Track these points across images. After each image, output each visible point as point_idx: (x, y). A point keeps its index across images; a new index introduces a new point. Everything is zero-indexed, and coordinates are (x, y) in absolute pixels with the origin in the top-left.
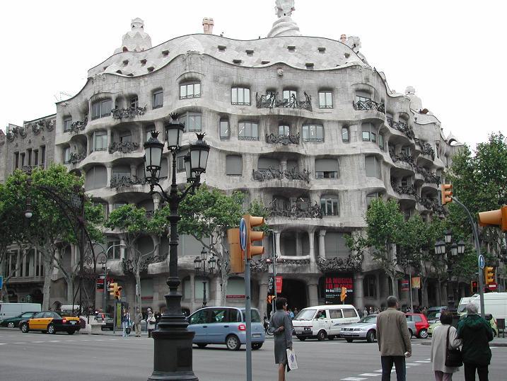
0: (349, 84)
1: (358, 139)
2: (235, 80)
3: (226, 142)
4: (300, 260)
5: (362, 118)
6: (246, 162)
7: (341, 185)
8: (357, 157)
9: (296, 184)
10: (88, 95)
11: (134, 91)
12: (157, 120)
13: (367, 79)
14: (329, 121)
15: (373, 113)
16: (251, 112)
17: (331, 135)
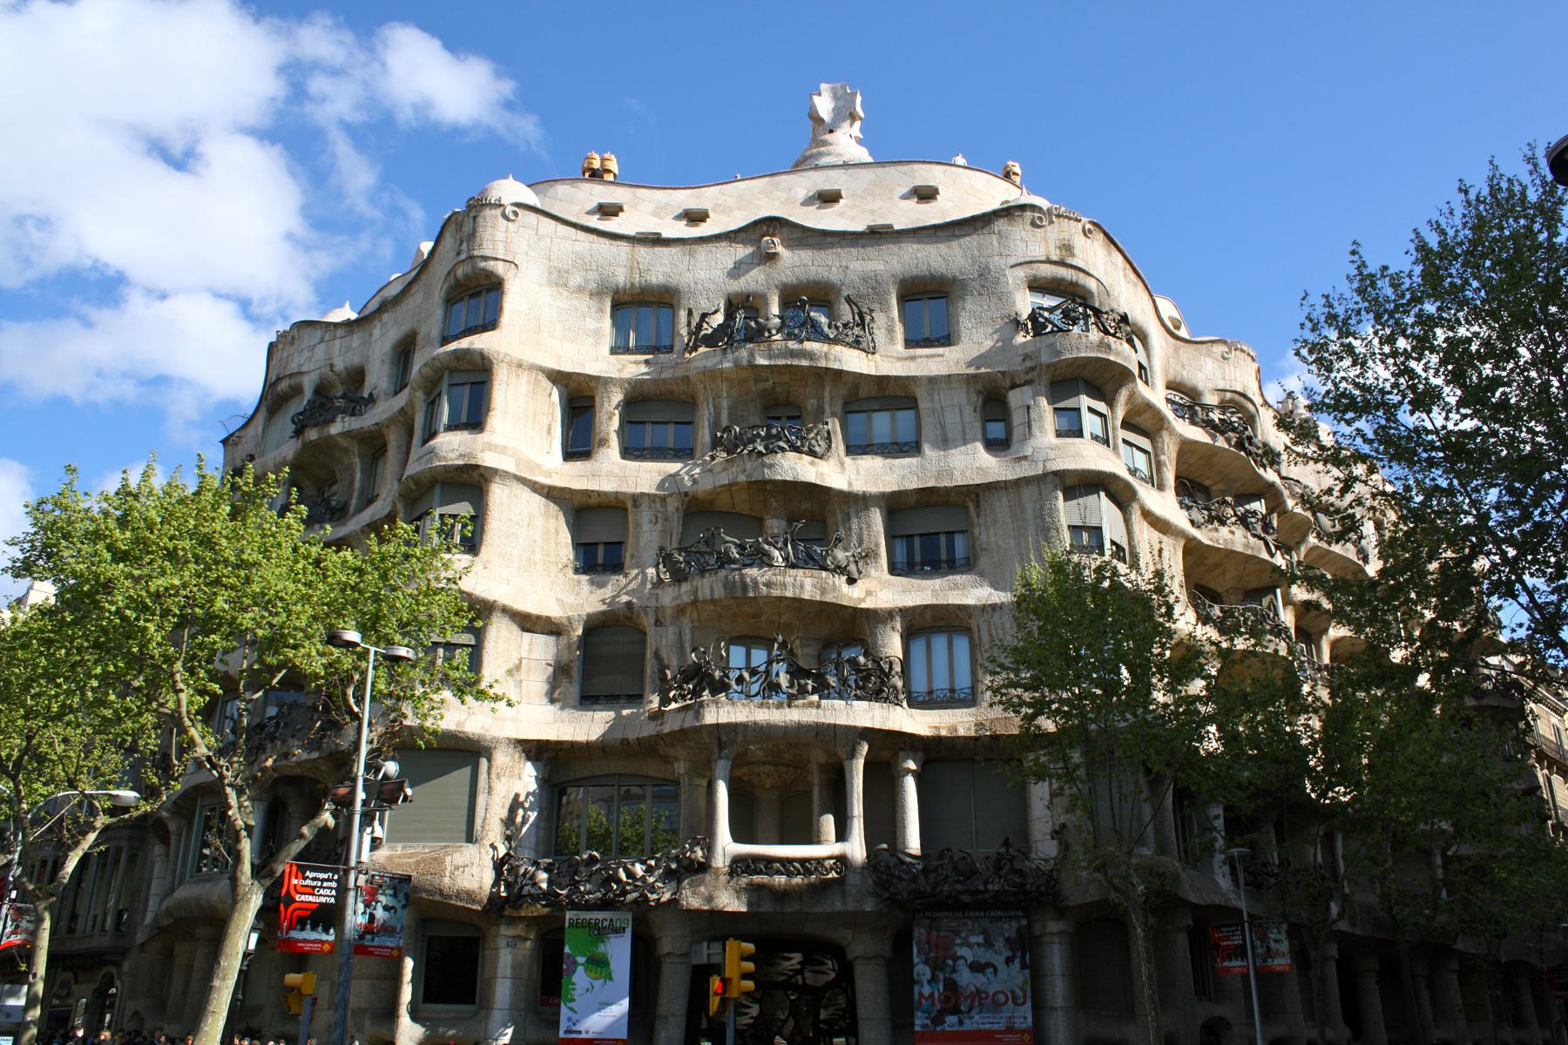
0: (997, 262)
2: (621, 278)
3: (578, 466)
4: (808, 860)
6: (638, 525)
11: (355, 359)
12: (392, 420)
14: (932, 380)
17: (943, 426)
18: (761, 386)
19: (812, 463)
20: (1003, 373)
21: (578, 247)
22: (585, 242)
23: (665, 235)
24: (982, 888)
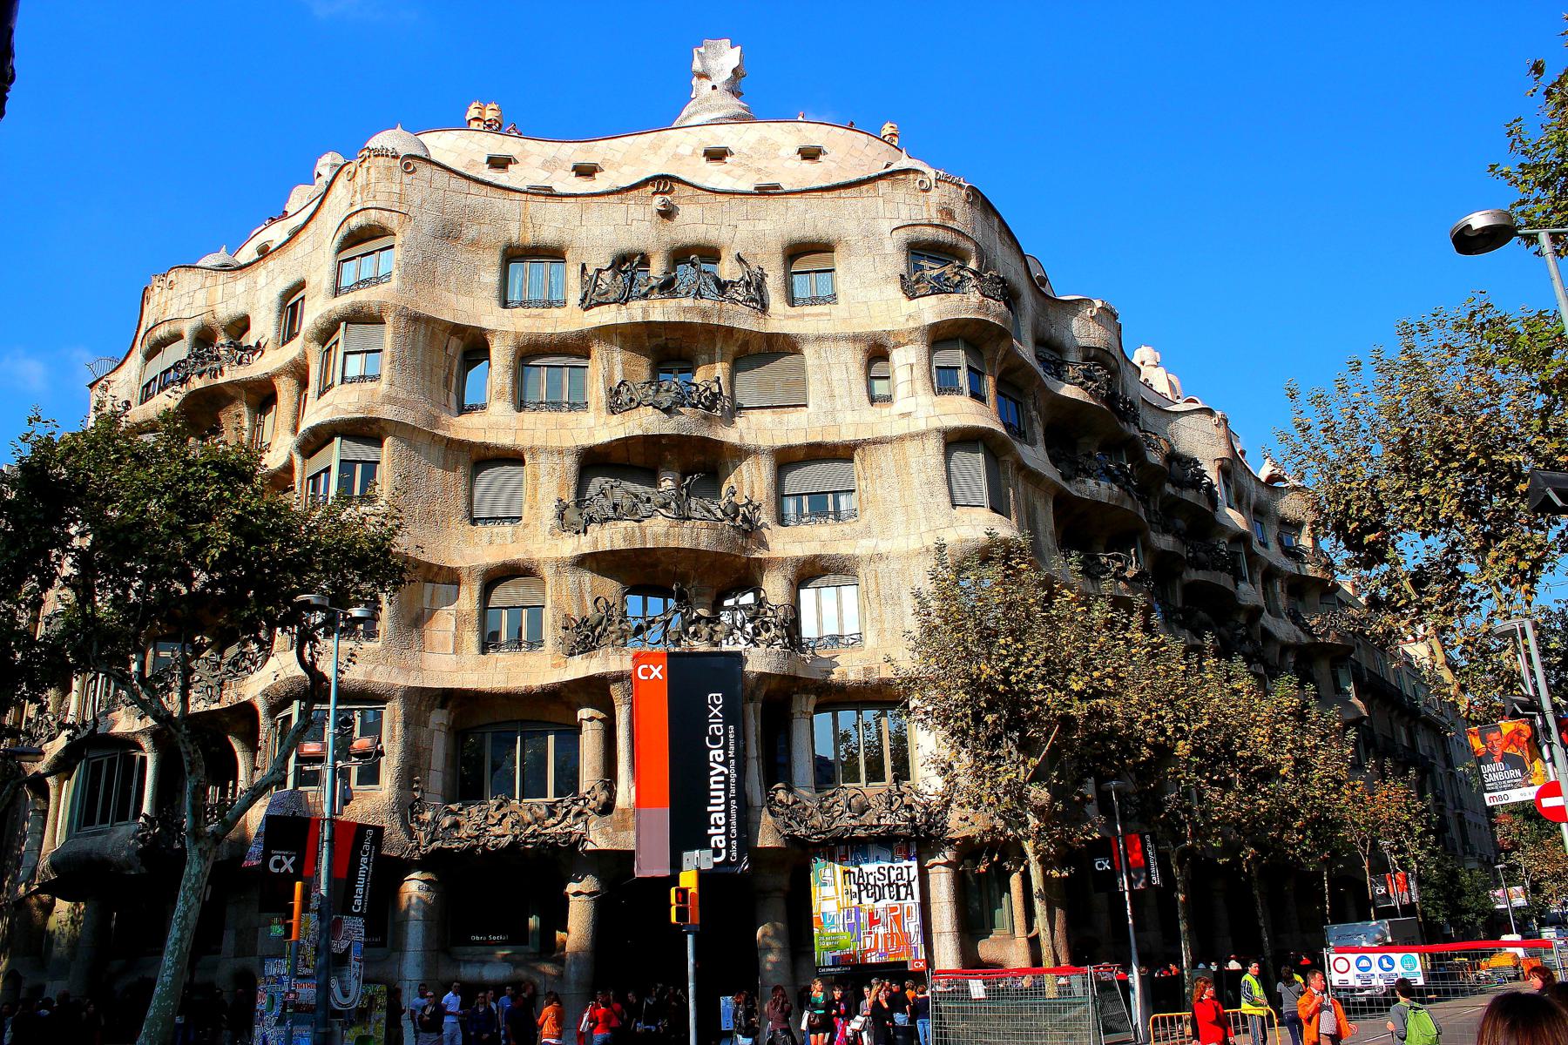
1: (919, 385)
2: (515, 233)
5: (930, 318)
6: (535, 477)
8: (917, 443)
9: (695, 535)
14: (820, 339)
15: (966, 304)
18: (655, 341)
19: (705, 418)
21: (471, 200)
22: (478, 196)
23: (559, 189)
24: (875, 822)
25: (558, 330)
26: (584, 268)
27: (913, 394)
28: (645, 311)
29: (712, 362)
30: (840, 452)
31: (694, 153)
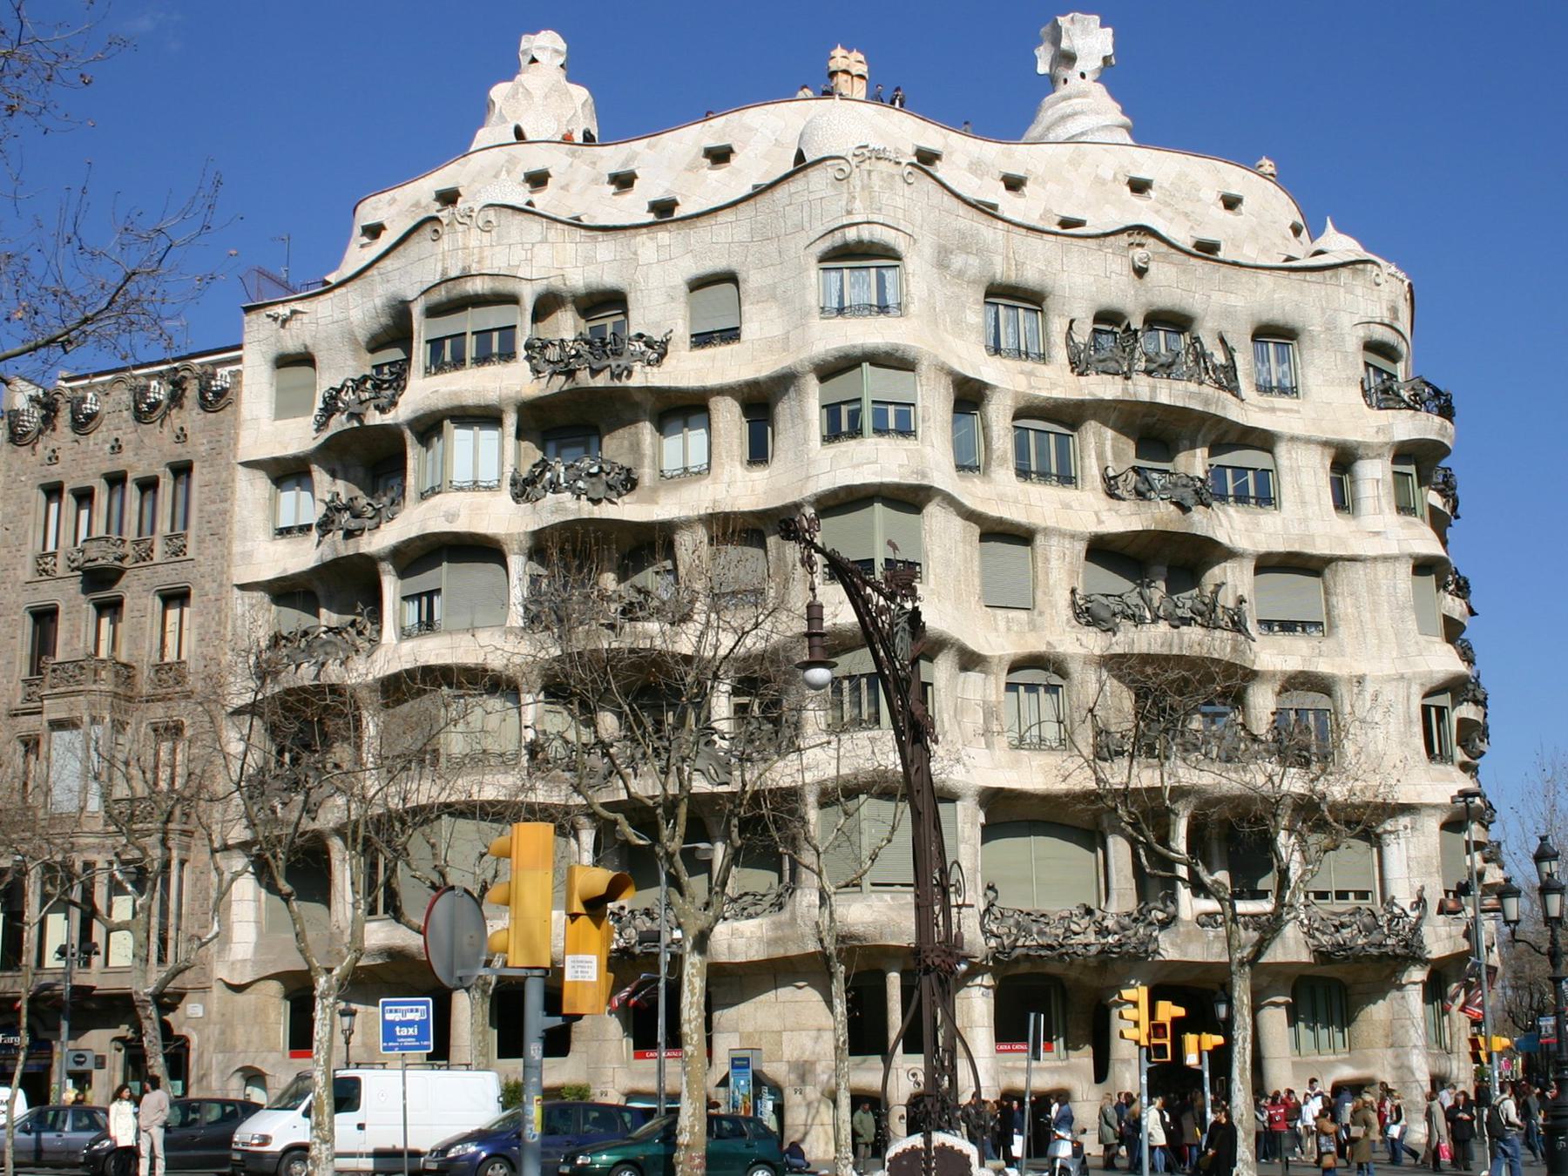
0: (1345, 321)
1: (1384, 501)
6: (1047, 560)
7: (1338, 660)
10: (412, 276)
13: (1394, 311)
14: (1293, 439)
16: (1054, 385)
20: (1359, 443)
25: (1059, 394)
26: (1072, 321)
27: (1381, 512)
28: (1153, 389)
29: (1193, 447)
30: (1312, 565)
31: (1115, 178)
